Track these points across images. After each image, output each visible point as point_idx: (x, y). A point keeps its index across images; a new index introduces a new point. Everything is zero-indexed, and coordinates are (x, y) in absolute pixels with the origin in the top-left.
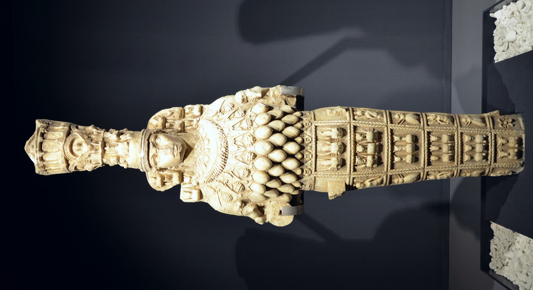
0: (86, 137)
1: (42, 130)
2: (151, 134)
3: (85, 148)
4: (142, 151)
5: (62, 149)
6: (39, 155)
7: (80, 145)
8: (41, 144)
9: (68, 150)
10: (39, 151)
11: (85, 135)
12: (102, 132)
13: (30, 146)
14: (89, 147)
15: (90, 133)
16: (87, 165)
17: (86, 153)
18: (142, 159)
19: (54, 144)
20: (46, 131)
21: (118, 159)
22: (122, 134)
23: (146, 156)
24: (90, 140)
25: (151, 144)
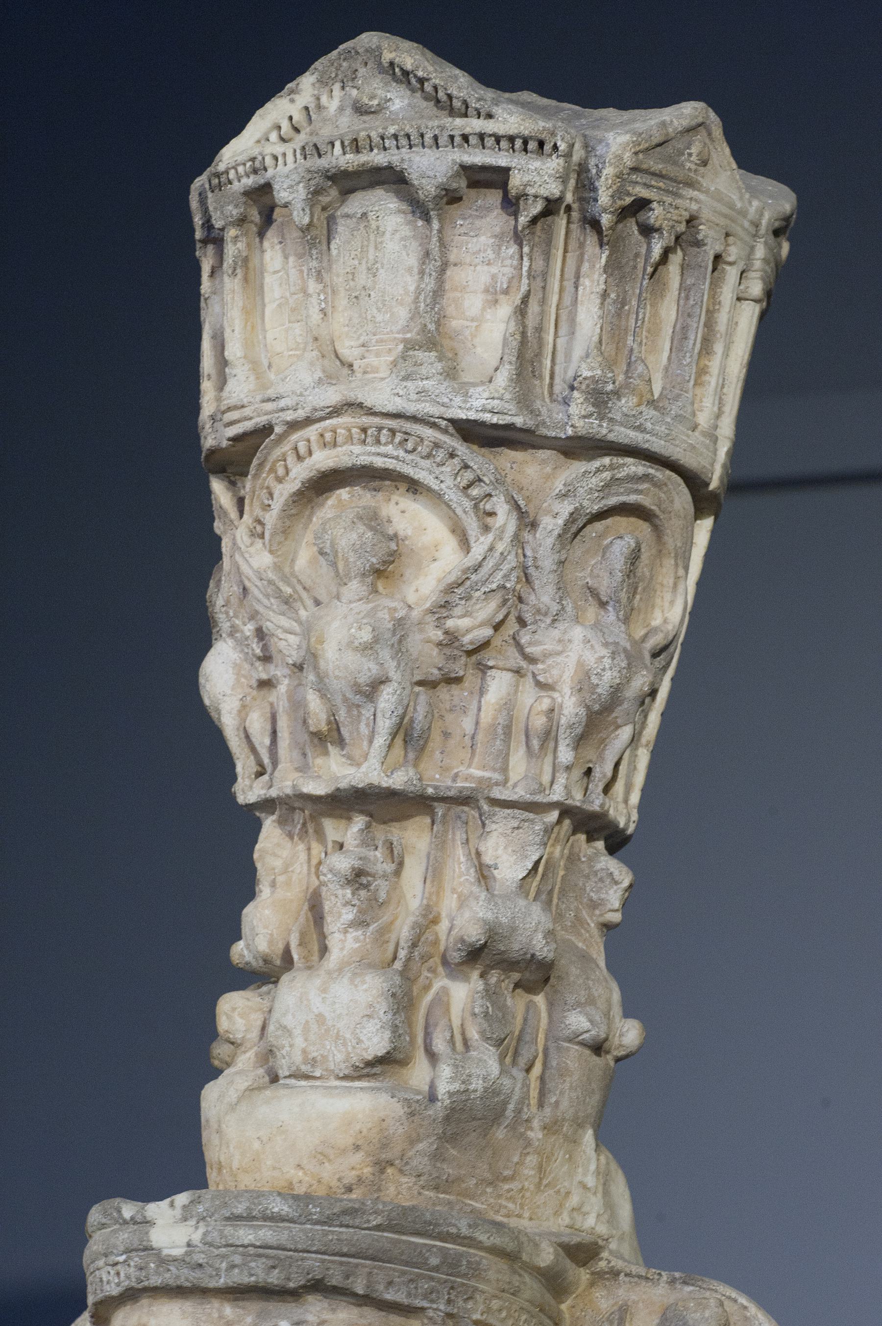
0: (472, 622)
1: (538, 176)
7: (386, 567)
11: (488, 610)
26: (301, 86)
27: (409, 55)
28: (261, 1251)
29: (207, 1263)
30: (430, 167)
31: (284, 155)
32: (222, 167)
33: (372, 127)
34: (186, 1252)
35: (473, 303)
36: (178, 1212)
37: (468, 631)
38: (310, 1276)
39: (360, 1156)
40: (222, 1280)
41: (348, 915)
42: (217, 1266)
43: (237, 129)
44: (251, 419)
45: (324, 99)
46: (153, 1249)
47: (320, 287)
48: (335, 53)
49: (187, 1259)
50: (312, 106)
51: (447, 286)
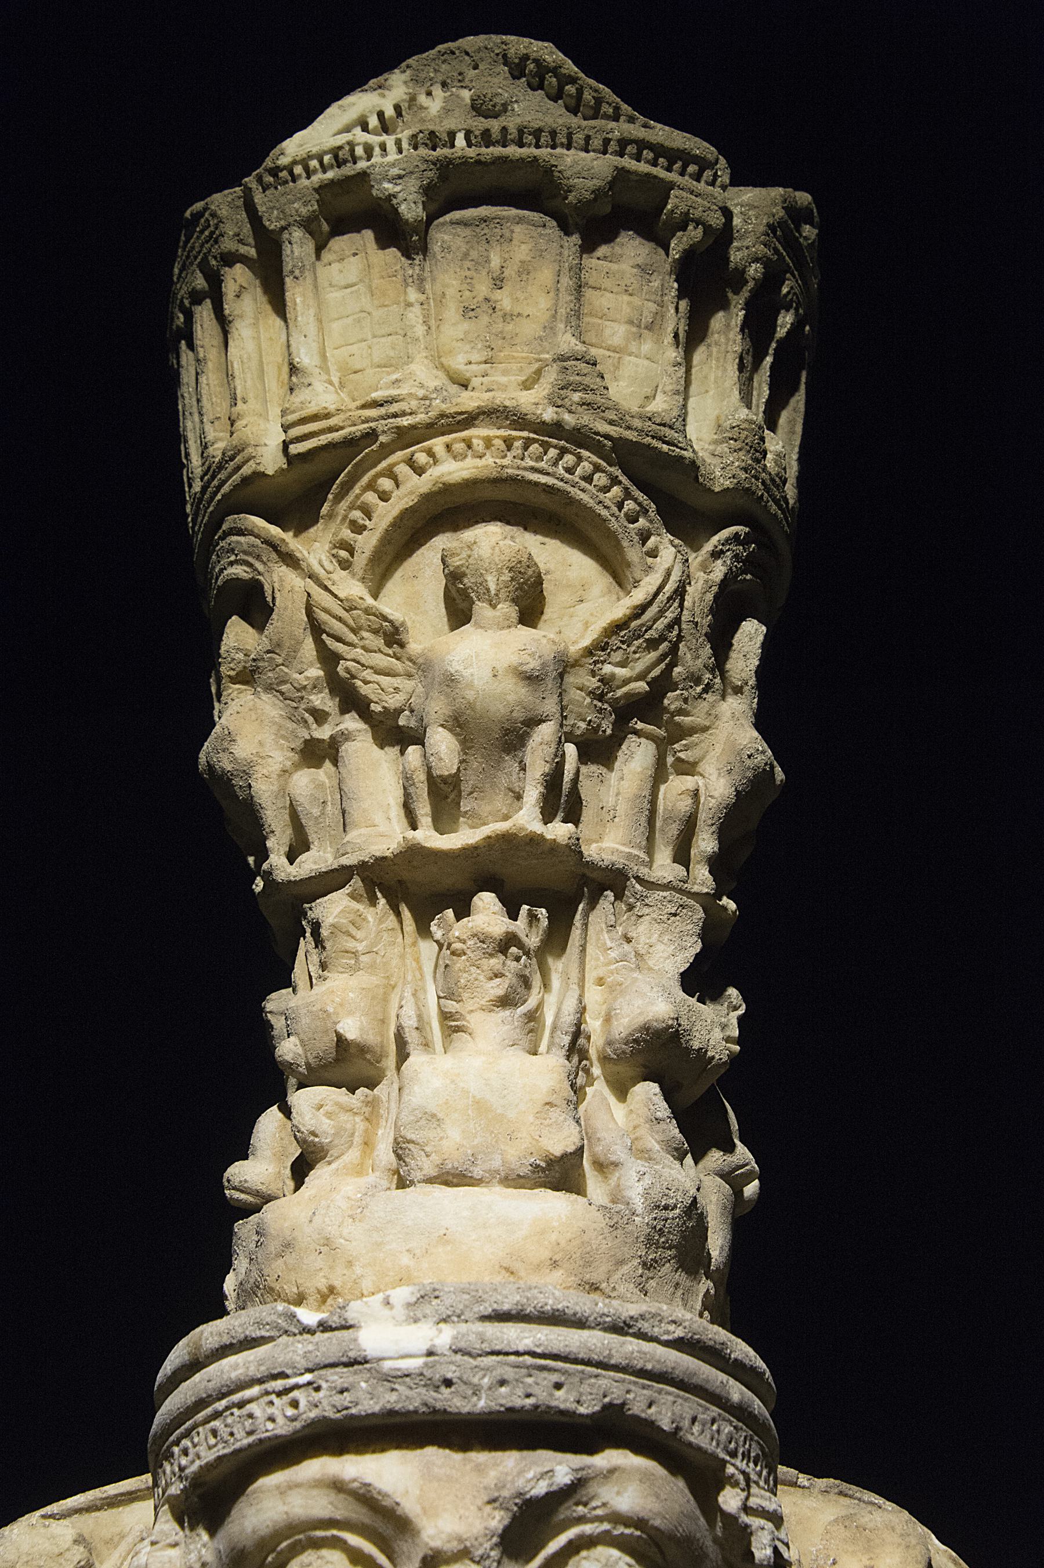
2: (702, 1476)
3: (487, 656)
4: (444, 1337)
5: (469, 401)
6: (395, 169)
8: (531, 190)
9: (452, 466)
10: (445, 168)
12: (702, 879)
13: (499, 84)
14: (505, 697)
15: (680, 733)
16: (270, 707)
17: (422, 667)
18: (328, 1345)
19: (529, 329)
20: (678, 245)
21: (348, 1066)
22: (698, 1133)
23: (368, 1400)
24: (585, 714)
25: (561, 1468)
26: (390, 82)
27: (547, 52)
28: (542, 1362)
29: (460, 1378)
30: (584, 169)
31: (383, 147)
32: (284, 161)
33: (495, 126)
34: (426, 1364)
35: (617, 333)
36: (399, 1311)
37: (626, 682)
38: (607, 1400)
39: (558, 1275)
40: (482, 1404)
41: (497, 988)
42: (475, 1380)
43: (304, 122)
44: (342, 428)
45: (422, 99)
46: (366, 1362)
47: (423, 297)
48: (432, 53)
49: (428, 1373)
50: (404, 106)
51: (585, 310)
